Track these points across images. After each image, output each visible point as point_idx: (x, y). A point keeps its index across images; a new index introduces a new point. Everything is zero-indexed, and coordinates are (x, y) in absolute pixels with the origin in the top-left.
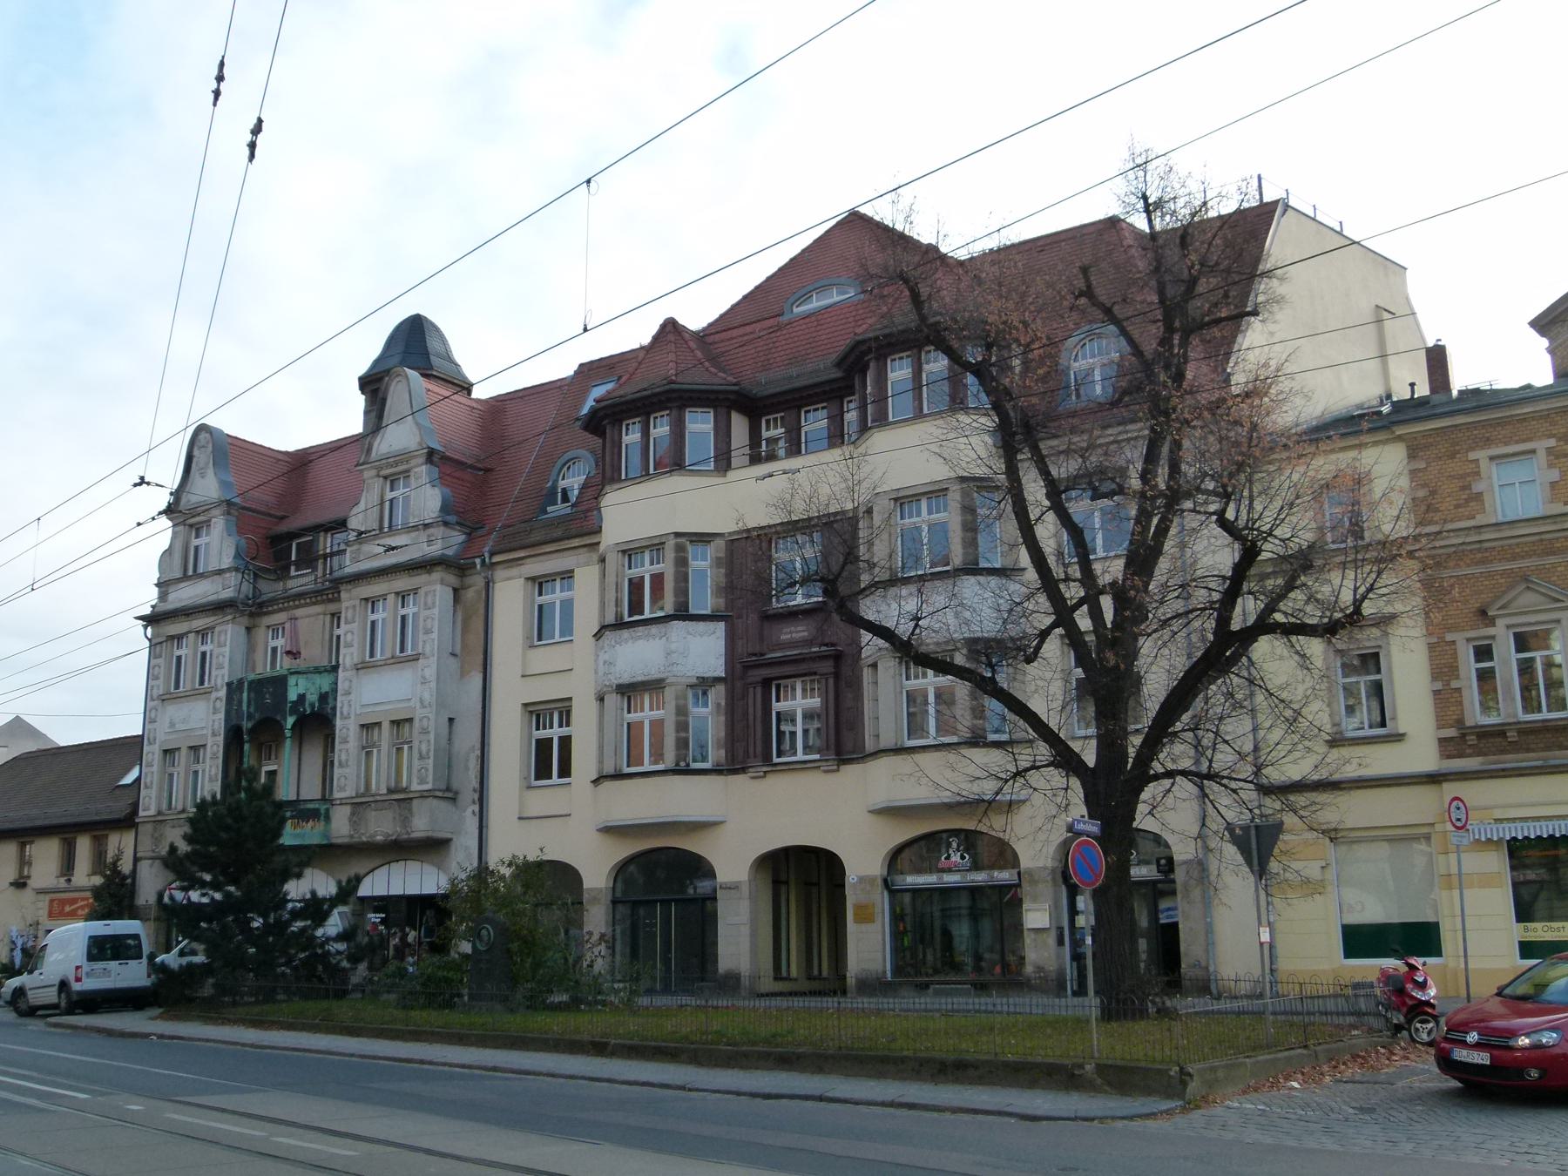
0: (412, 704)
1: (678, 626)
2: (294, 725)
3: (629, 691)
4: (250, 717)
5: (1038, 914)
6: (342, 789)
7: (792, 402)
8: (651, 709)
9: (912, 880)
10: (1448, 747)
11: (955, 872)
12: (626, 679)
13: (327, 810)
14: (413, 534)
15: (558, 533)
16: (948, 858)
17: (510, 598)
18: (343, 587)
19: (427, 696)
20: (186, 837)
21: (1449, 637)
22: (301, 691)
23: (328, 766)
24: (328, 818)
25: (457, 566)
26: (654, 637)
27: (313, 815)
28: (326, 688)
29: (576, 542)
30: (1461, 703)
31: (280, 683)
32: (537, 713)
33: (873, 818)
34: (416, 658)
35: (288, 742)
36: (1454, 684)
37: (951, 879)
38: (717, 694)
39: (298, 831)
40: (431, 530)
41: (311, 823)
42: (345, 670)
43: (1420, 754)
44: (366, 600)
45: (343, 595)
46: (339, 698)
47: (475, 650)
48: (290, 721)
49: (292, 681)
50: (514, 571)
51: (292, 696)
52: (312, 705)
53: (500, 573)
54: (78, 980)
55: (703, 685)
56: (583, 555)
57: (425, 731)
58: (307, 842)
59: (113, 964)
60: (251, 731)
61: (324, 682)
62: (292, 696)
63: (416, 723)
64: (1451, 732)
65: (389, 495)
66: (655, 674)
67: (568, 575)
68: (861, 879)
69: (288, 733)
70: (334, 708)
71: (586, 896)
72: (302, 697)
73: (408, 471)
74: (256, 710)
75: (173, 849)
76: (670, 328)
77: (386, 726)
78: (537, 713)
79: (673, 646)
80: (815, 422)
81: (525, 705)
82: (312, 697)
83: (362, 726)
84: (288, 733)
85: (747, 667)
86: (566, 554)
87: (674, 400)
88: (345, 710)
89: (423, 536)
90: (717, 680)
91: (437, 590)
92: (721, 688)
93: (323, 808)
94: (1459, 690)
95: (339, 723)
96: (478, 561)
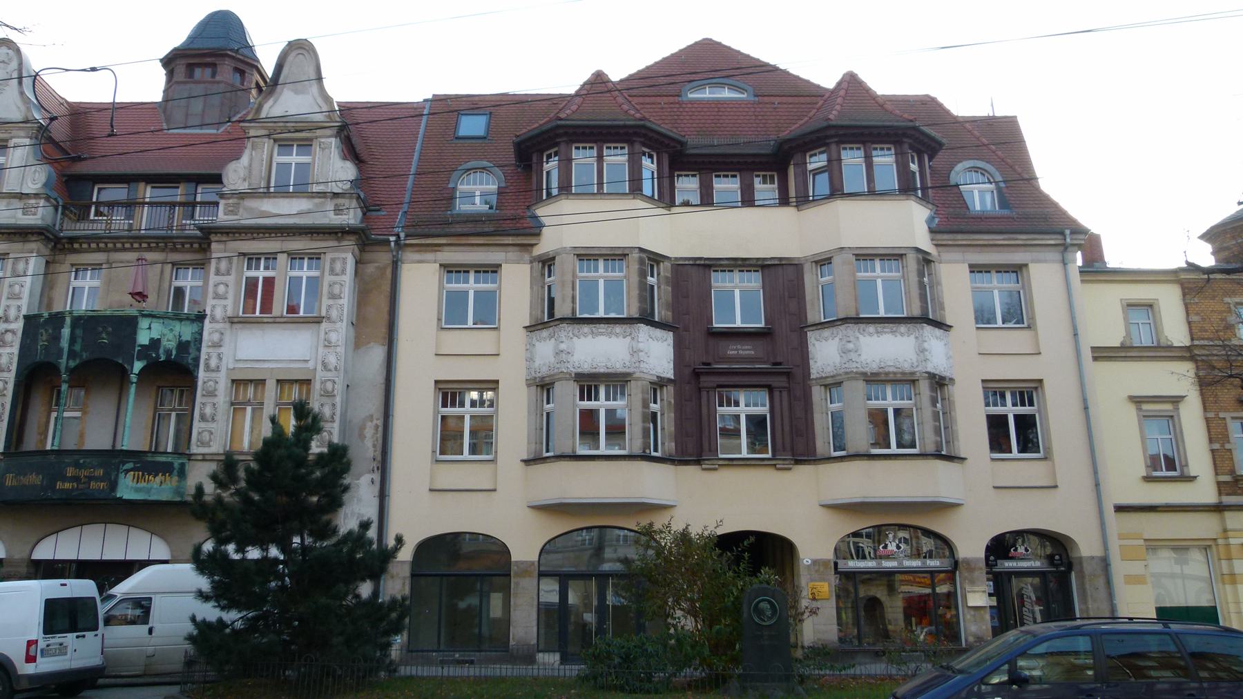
0: (311, 365)
1: (643, 328)
2: (142, 370)
3: (588, 383)
4: (72, 354)
5: (977, 595)
6: (203, 443)
7: (708, 165)
8: (608, 399)
9: (854, 564)
10: (1221, 487)
11: (897, 556)
12: (586, 368)
13: (183, 465)
14: (317, 201)
15: (488, 228)
16: (885, 547)
17: (421, 282)
18: (213, 237)
19: (332, 360)
20: (214, 477)
21: (1222, 415)
22: (156, 336)
23: (185, 422)
24: (182, 473)
25: (363, 239)
26: (617, 335)
27: (166, 469)
28: (187, 337)
29: (510, 240)
30: (1232, 459)
31: (129, 324)
32: (449, 393)
33: (531, 514)
34: (318, 321)
35: (133, 389)
36: (1227, 446)
37: (889, 564)
38: (668, 393)
39: (142, 485)
40: (340, 201)
41: (159, 479)
42: (213, 320)
43: (1204, 491)
44: (244, 254)
45: (214, 246)
46: (204, 350)
47: (379, 319)
48: (138, 366)
49: (144, 323)
50: (429, 256)
51: (143, 338)
52: (168, 352)
53: (409, 255)
54: (30, 659)
55: (659, 384)
56: (512, 254)
57: (329, 395)
58: (154, 497)
59: (71, 637)
60: (72, 371)
61: (186, 331)
62: (143, 338)
63: (317, 386)
64: (1227, 478)
65: (278, 159)
66: (619, 368)
67: (494, 269)
68: (815, 562)
69: (134, 378)
70: (197, 359)
71: (514, 568)
72: (155, 343)
73: (311, 140)
74: (83, 349)
75: (200, 490)
76: (599, 79)
77: (271, 386)
78: (449, 393)
79: (563, 346)
80: (726, 186)
81: (437, 382)
82: (169, 343)
83: (233, 381)
84: (134, 378)
85: (697, 374)
86: (492, 248)
87: (600, 135)
88: (213, 363)
89: (330, 205)
90: (669, 380)
91: (345, 257)
92: (671, 388)
93: (177, 463)
94: (1230, 450)
95: (202, 374)
96: (392, 239)
